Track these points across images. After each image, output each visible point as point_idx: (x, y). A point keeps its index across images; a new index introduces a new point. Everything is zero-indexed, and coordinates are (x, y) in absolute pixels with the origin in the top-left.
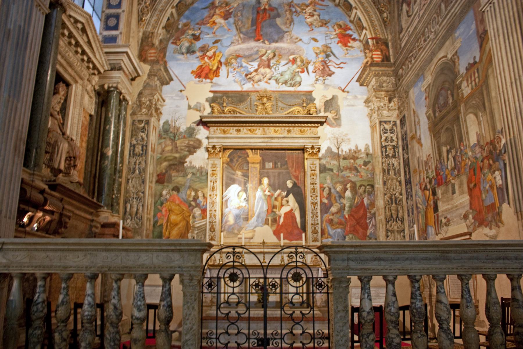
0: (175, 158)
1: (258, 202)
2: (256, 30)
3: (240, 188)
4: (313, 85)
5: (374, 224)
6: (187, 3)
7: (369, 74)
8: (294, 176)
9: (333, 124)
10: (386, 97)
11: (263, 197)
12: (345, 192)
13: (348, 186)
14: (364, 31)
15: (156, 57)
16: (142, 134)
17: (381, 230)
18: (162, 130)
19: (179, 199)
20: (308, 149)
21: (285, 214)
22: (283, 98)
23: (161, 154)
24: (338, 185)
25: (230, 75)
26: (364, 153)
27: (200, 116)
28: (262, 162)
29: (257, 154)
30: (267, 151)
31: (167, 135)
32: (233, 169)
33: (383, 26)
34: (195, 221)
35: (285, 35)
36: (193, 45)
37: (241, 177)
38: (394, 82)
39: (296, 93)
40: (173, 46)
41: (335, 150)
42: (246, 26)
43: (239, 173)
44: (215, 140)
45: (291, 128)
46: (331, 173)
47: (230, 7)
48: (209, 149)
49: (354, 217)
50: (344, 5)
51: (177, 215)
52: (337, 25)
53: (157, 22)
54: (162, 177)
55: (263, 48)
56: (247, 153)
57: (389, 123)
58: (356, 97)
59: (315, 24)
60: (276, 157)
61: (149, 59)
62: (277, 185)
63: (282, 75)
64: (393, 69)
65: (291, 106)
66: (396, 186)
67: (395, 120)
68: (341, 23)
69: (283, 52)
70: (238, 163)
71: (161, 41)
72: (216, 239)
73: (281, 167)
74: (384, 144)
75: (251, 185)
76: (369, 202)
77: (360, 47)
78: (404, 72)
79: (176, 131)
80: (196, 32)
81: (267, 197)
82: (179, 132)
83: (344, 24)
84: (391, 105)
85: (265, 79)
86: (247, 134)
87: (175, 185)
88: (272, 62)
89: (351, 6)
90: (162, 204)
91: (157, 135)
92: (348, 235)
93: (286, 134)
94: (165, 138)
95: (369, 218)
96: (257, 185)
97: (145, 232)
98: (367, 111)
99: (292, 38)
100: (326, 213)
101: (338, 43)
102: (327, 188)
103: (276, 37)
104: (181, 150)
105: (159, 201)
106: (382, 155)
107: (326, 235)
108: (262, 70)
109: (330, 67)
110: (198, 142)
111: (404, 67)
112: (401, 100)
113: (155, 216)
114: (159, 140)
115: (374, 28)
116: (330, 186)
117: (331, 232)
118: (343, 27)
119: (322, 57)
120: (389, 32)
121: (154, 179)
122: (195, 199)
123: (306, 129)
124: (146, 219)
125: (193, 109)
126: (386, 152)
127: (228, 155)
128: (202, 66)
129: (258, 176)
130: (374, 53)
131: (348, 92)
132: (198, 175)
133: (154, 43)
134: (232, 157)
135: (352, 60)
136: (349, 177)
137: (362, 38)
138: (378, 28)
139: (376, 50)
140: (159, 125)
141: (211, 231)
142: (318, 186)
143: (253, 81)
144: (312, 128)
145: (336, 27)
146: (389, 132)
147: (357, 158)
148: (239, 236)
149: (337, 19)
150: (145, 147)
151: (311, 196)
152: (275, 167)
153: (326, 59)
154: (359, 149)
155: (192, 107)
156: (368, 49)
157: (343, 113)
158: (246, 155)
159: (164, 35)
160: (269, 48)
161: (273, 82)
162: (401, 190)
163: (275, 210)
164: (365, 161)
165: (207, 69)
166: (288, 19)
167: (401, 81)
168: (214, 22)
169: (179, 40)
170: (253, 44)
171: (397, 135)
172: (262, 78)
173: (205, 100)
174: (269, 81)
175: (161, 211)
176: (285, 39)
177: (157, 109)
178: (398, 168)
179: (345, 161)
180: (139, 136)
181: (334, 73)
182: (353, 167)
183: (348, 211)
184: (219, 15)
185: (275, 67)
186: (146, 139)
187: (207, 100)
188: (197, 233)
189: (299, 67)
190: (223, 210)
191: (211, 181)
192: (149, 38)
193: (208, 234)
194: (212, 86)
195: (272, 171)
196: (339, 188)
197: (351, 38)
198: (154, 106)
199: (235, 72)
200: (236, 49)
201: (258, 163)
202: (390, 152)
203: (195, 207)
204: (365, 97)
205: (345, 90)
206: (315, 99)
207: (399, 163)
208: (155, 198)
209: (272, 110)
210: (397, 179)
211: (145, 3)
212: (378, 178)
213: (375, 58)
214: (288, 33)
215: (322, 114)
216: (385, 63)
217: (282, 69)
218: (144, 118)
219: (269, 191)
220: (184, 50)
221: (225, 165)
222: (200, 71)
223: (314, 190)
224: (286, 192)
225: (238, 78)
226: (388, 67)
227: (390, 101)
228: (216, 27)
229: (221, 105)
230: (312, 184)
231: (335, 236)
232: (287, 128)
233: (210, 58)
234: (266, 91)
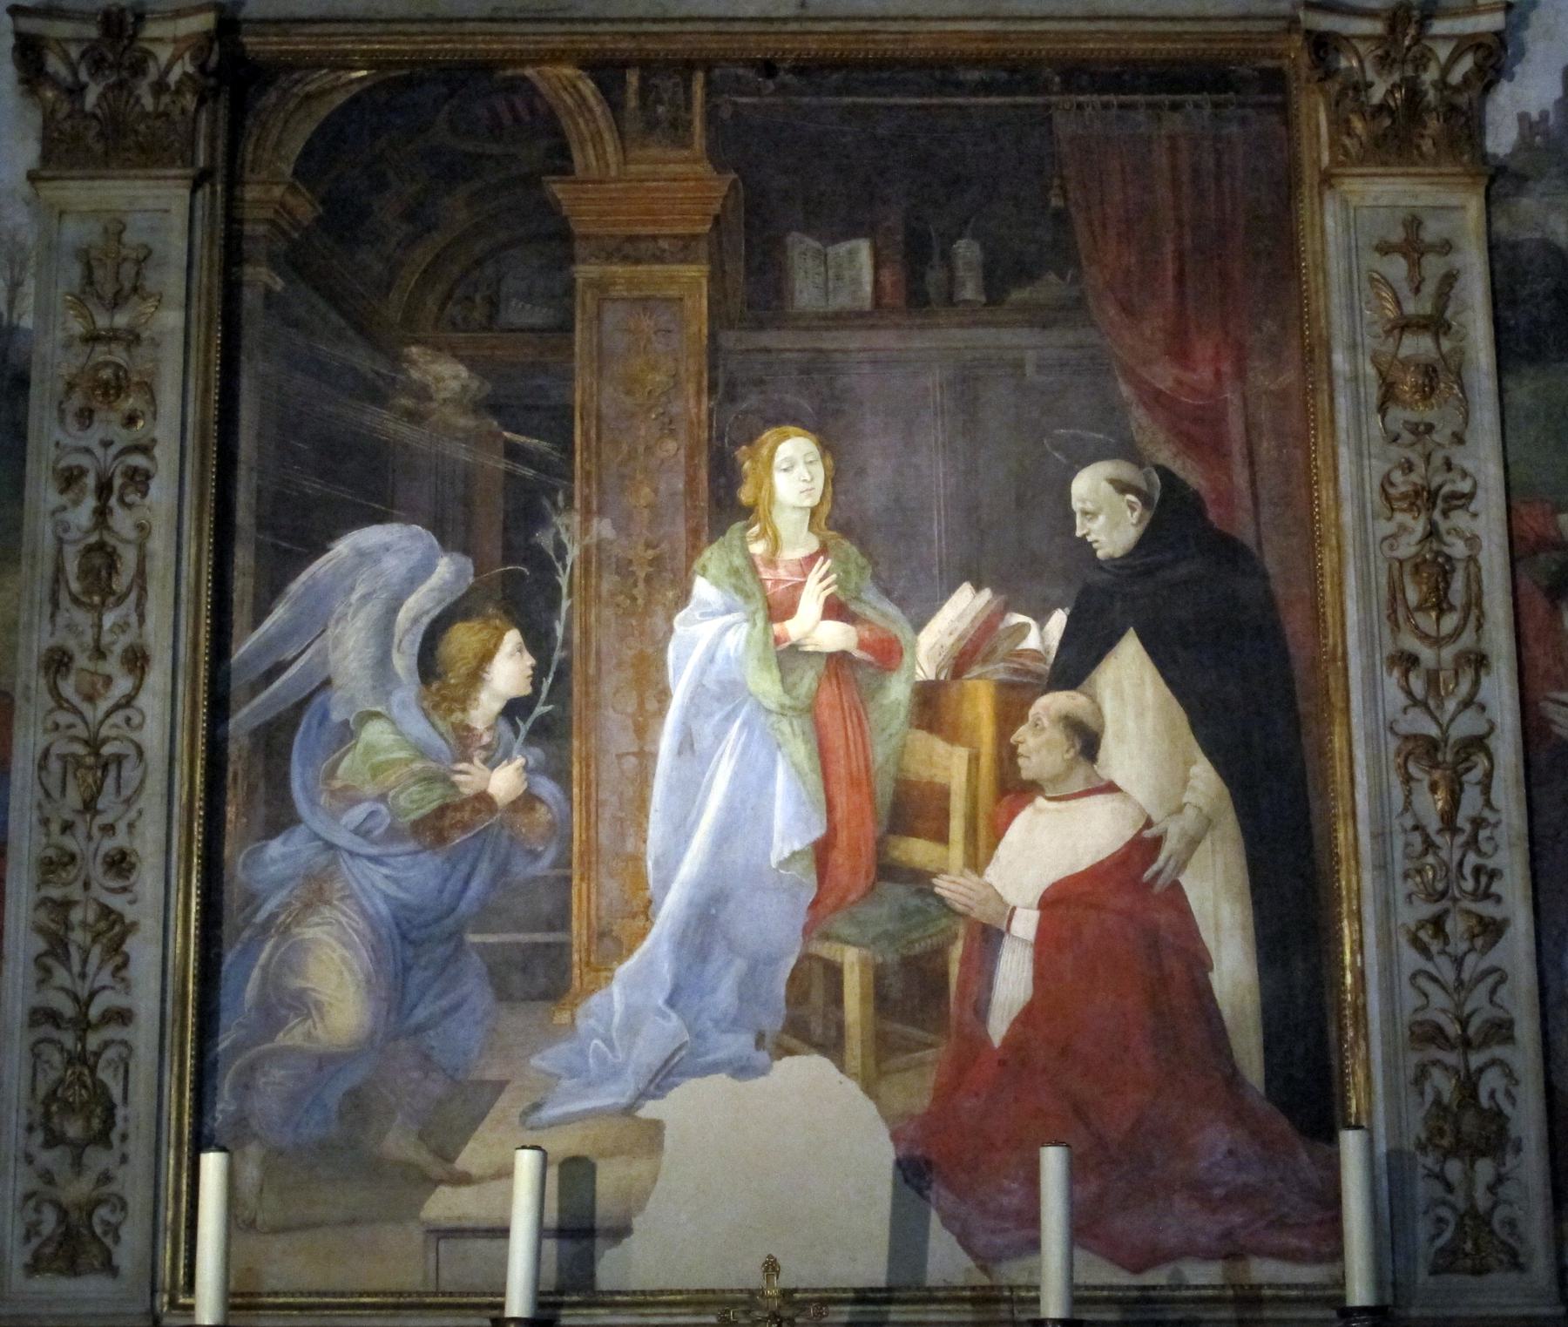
1: (687, 744)
8: (1155, 400)
11: (766, 685)
29: (677, 131)
32: (365, 329)
37: (465, 422)
70: (438, 239)
73: (994, 291)
75: (603, 528)
81: (807, 680)
96: (681, 529)
127: (296, 146)
129: (693, 406)
141: (54, 1139)
148: (445, 1204)
151: (1408, 661)
163: (918, 851)
191: (69, 479)
195: (885, 339)
201: (685, 248)
219: (835, 609)
224: (1058, 621)
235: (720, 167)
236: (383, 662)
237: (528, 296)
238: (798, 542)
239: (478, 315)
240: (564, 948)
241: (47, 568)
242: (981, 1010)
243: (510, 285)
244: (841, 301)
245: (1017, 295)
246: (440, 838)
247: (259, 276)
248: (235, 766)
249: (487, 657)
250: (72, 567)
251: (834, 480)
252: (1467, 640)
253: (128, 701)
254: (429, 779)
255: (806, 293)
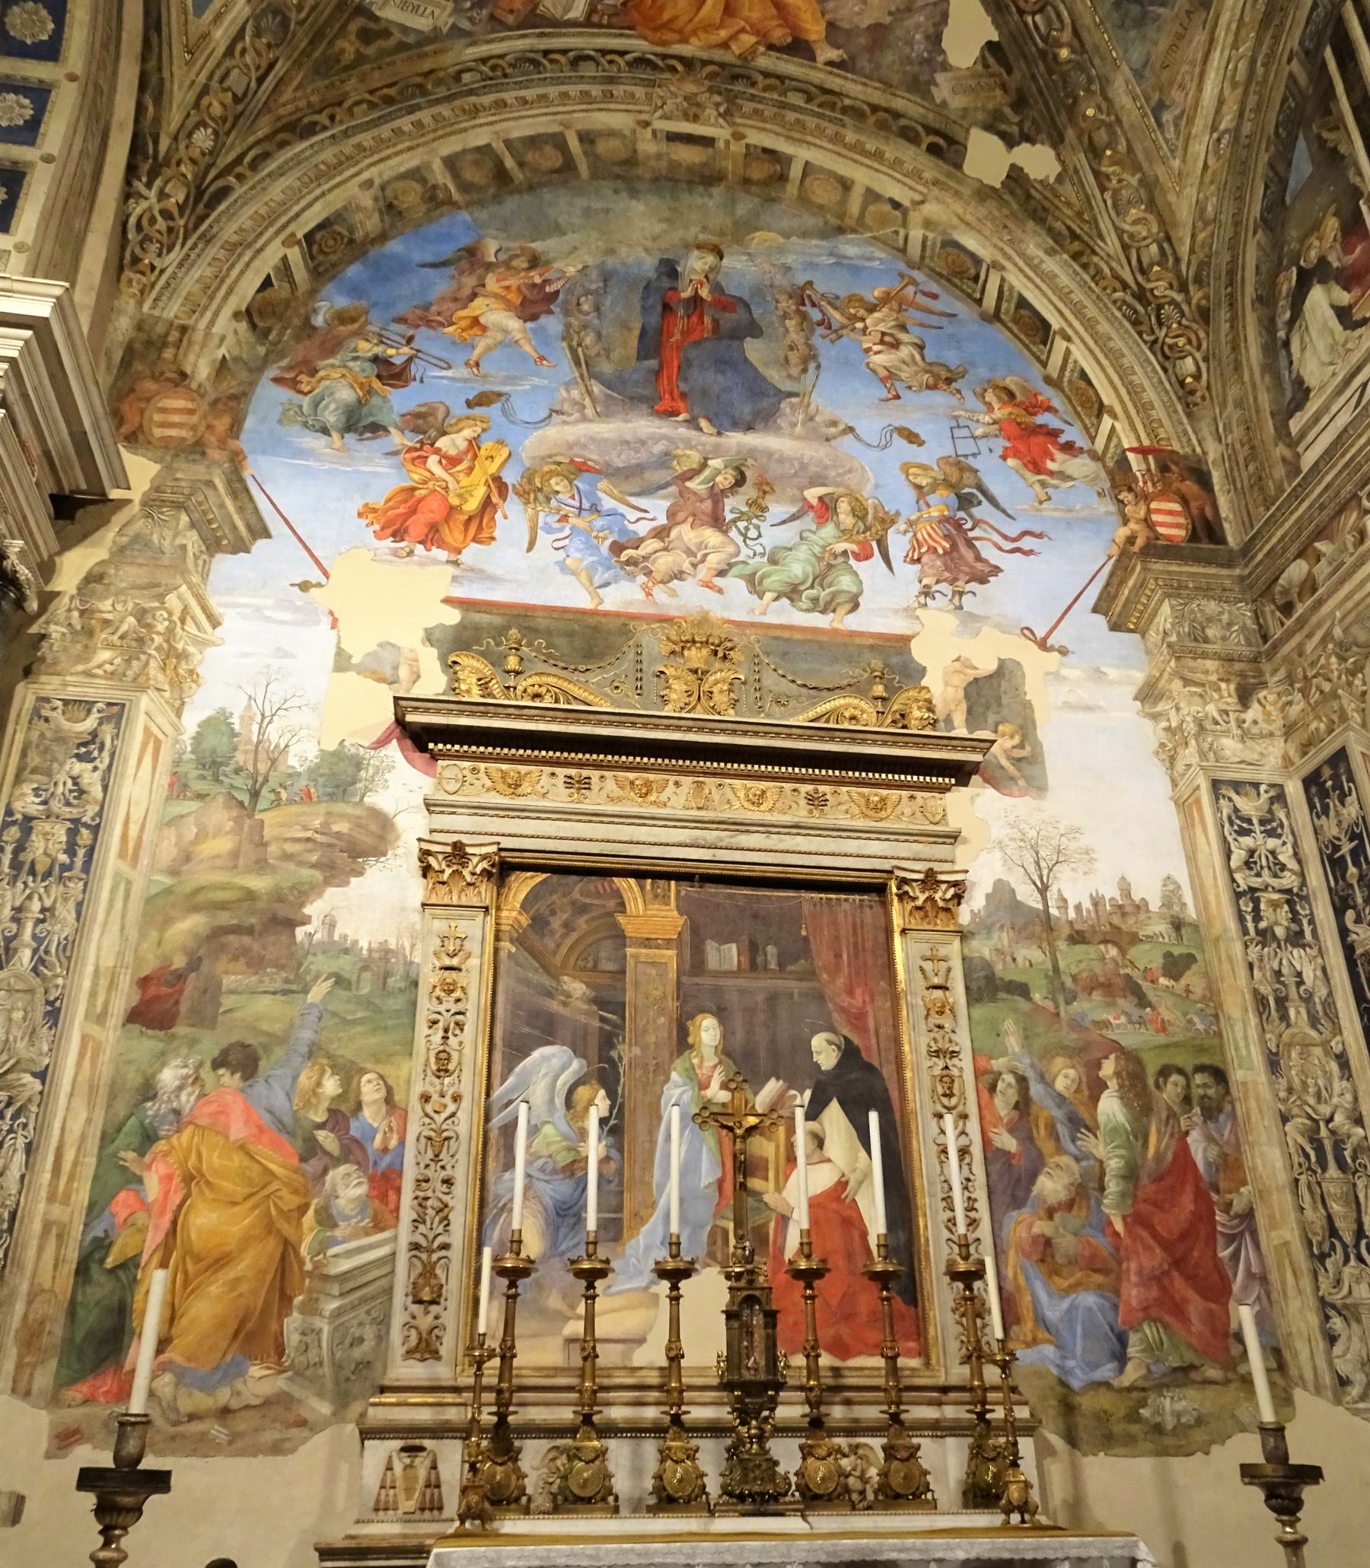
0: (250, 895)
2: (658, 373)
3: (576, 1064)
4: (909, 612)
5: (1255, 1269)
6: (359, 235)
7: (1142, 585)
8: (843, 1010)
9: (1012, 779)
10: (1228, 681)
12: (1095, 1099)
13: (1108, 1068)
14: (1107, 422)
15: (194, 428)
16: (78, 767)
17: (1294, 1305)
18: (188, 756)
19: (247, 1110)
20: (906, 888)
21: (816, 1204)
22: (784, 655)
23: (174, 872)
24: (1059, 1061)
25: (544, 539)
26: (1162, 916)
27: (396, 699)
28: (687, 937)
30: (711, 889)
31: (217, 780)
32: (547, 970)
33: (1179, 408)
34: (335, 1242)
35: (784, 405)
36: (375, 401)
37: (585, 1007)
38: (1249, 622)
39: (839, 639)
40: (284, 394)
41: (1028, 896)
42: (615, 355)
43: (577, 988)
44: (462, 822)
45: (822, 788)
46: (1021, 1003)
47: (547, 276)
48: (432, 860)
49: (1149, 1227)
50: (1016, 320)
51: (234, 1204)
52: (996, 387)
53: (209, 289)
54: (164, 990)
55: (691, 448)
56: (617, 894)
57: (1253, 792)
58: (1098, 674)
59: (903, 375)
60: (755, 916)
61: (158, 432)
62: (762, 1053)
63: (773, 561)
64: (1237, 571)
65: (820, 691)
66: (1329, 1079)
67: (1278, 780)
68: (1010, 382)
69: (775, 470)
70: (575, 936)
71: (222, 367)
72: (443, 1351)
73: (781, 965)
74: (1243, 880)
76: (1213, 1152)
77: (1097, 477)
78: (1322, 569)
79: (262, 767)
80: (391, 352)
82: (282, 768)
83: (1024, 389)
84: (1249, 715)
85: (703, 572)
86: (619, 799)
87: (234, 1038)
88: (732, 505)
89: (1046, 326)
90: (148, 1138)
91: (163, 779)
92: (1137, 1328)
93: (801, 813)
94: (200, 797)
95: (1231, 1239)
97: (19, 1308)
98: (1150, 733)
99: (812, 419)
100: (1018, 1202)
101: (1004, 457)
102: (1009, 1078)
103: (746, 410)
104: (287, 857)
105: (133, 1120)
106: (1245, 932)
107: (1028, 1325)
108: (686, 533)
109: (977, 543)
110: (373, 828)
111: (1321, 546)
112: (1305, 693)
113: (94, 1209)
114: (169, 798)
115: (1145, 410)
116: (1024, 1066)
117: (1054, 1311)
118: (1019, 397)
119: (940, 503)
120: (1206, 431)
121: (123, 1000)
122: (339, 1117)
123: (894, 794)
124: (37, 1227)
125: (362, 670)
126: (1257, 917)
127: (522, 897)
128: (414, 489)
129: (672, 1005)
130: (1154, 505)
131: (1063, 652)
132: (365, 990)
133: (188, 371)
134: (541, 907)
135: (1069, 524)
136: (1106, 1024)
137: (1100, 444)
138: (1159, 412)
139: (1161, 495)
140: (178, 730)
142: (965, 1064)
143: (649, 573)
144: (919, 794)
145: (990, 397)
146: (1257, 828)
147: (1134, 939)
149: (992, 369)
150: (85, 832)
152: (753, 963)
153: (961, 514)
154: (1136, 897)
155: (354, 661)
156: (1130, 490)
157: (1049, 732)
158: (611, 904)
159: (239, 342)
160: (717, 451)
161: (735, 585)
162: (1356, 1099)
163: (755, 1183)
164: (1168, 955)
165: (434, 503)
166: (791, 348)
167: (1300, 609)
168: (475, 321)
169: (313, 372)
170: (644, 426)
171: (1295, 845)
172: (686, 566)
173: (421, 634)
174: (719, 582)
175: (140, 1180)
176: (782, 422)
177: (173, 655)
178: (1322, 992)
179: (1080, 948)
180: (62, 777)
181: (996, 570)
182: (1118, 981)
183: (1123, 1195)
184: (496, 296)
185: (742, 525)
186: (97, 792)
187: (430, 637)
188: (338, 1313)
189: (845, 533)
190: (491, 1178)
192: (165, 344)
193: (398, 1319)
194: (455, 579)
195: (740, 982)
196: (1065, 1077)
197: (1055, 444)
198: (158, 640)
199: (567, 532)
200: (571, 439)
202: (1279, 920)
203: (337, 1162)
204: (1139, 677)
205: (1050, 642)
206: (923, 671)
207: (1324, 970)
208: (109, 1106)
209: (734, 703)
210: (1325, 1045)
211: (162, 195)
212: (1239, 1035)
213: (1162, 524)
214: (794, 400)
215: (961, 732)
216: (1206, 546)
217: (773, 536)
218: (99, 691)
219: (724, 1086)
220: (331, 416)
221: (506, 945)
222: (402, 510)
223: (947, 1084)
224: (808, 1093)
225: (577, 556)
226: (1222, 566)
227: (1245, 697)
228: (482, 345)
229: (496, 660)
230: (937, 1053)
231: (1072, 1329)
232: (806, 788)
233: (451, 462)
234: (704, 620)
235: (681, 914)
236: (551, 1101)
237: (609, 959)
238: (711, 1059)
239: (590, 965)
240: (621, 1220)
241: (422, 1059)
242: (781, 1250)
243: (603, 954)
244: (725, 967)
245: (790, 968)
246: (572, 1175)
247: (506, 945)
248: (493, 1141)
249: (591, 1102)
250: (433, 1060)
251: (724, 1036)
252: (960, 1108)
253: (453, 1115)
254: (569, 1149)
255: (713, 961)
